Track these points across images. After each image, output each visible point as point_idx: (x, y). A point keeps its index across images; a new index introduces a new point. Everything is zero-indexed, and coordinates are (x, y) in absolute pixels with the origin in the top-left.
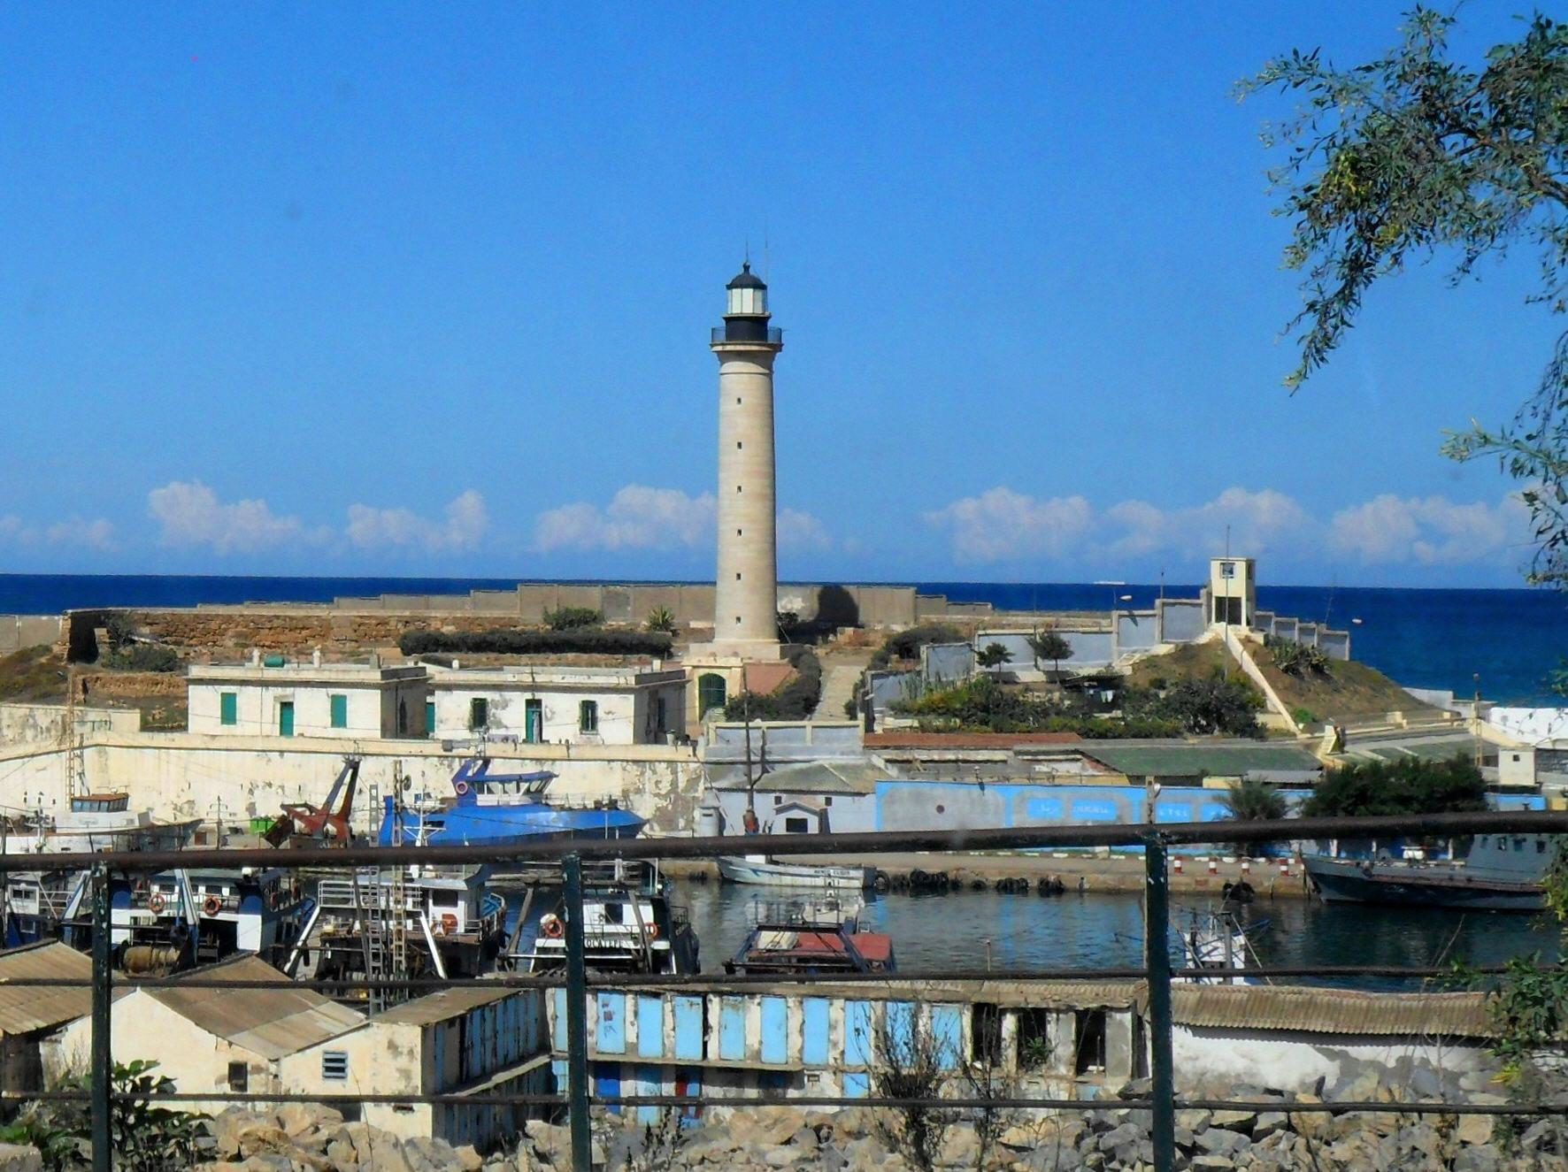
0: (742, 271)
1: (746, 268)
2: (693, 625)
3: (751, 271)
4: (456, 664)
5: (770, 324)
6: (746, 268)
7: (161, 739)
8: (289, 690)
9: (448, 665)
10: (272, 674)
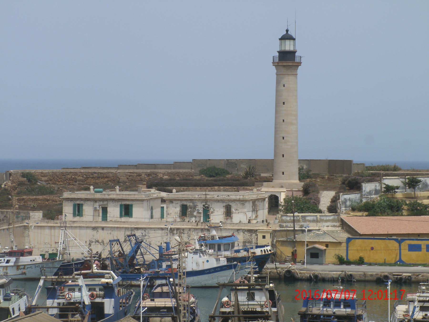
0: (285, 33)
1: (287, 31)
2: (262, 175)
3: (289, 33)
4: (174, 191)
5: (297, 54)
6: (287, 31)
7: (51, 223)
8: (105, 203)
9: (171, 191)
10: (98, 196)
